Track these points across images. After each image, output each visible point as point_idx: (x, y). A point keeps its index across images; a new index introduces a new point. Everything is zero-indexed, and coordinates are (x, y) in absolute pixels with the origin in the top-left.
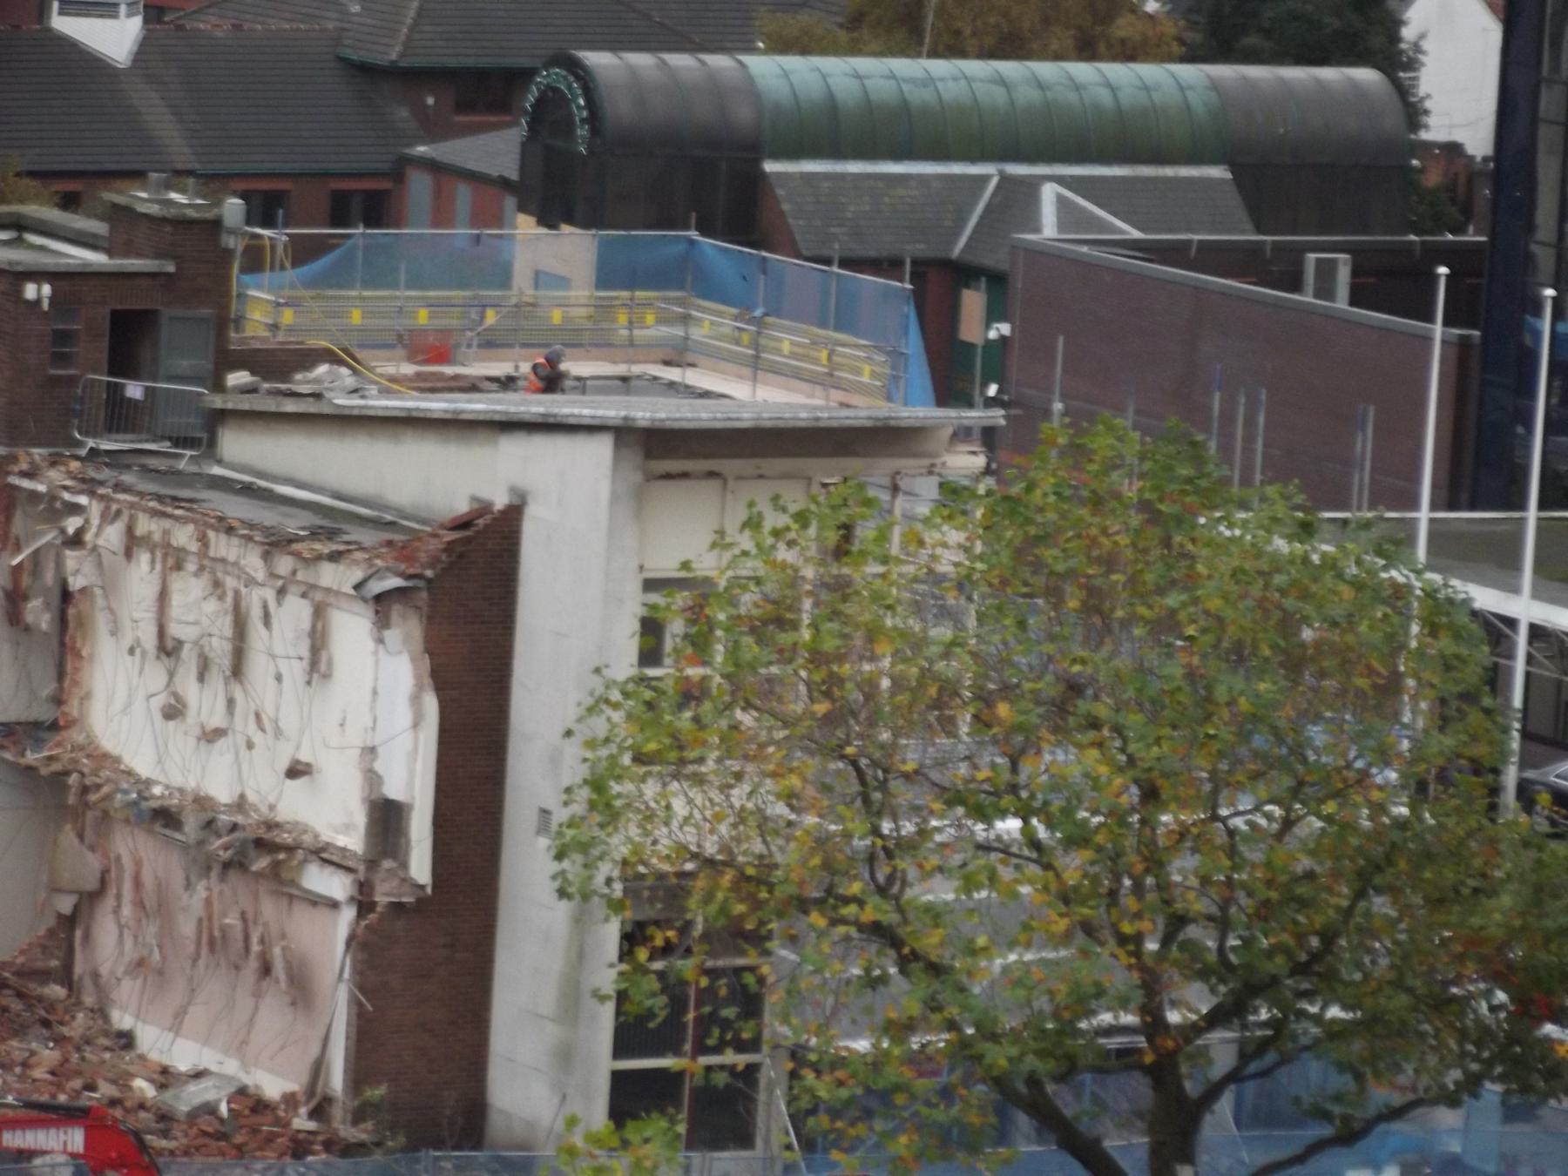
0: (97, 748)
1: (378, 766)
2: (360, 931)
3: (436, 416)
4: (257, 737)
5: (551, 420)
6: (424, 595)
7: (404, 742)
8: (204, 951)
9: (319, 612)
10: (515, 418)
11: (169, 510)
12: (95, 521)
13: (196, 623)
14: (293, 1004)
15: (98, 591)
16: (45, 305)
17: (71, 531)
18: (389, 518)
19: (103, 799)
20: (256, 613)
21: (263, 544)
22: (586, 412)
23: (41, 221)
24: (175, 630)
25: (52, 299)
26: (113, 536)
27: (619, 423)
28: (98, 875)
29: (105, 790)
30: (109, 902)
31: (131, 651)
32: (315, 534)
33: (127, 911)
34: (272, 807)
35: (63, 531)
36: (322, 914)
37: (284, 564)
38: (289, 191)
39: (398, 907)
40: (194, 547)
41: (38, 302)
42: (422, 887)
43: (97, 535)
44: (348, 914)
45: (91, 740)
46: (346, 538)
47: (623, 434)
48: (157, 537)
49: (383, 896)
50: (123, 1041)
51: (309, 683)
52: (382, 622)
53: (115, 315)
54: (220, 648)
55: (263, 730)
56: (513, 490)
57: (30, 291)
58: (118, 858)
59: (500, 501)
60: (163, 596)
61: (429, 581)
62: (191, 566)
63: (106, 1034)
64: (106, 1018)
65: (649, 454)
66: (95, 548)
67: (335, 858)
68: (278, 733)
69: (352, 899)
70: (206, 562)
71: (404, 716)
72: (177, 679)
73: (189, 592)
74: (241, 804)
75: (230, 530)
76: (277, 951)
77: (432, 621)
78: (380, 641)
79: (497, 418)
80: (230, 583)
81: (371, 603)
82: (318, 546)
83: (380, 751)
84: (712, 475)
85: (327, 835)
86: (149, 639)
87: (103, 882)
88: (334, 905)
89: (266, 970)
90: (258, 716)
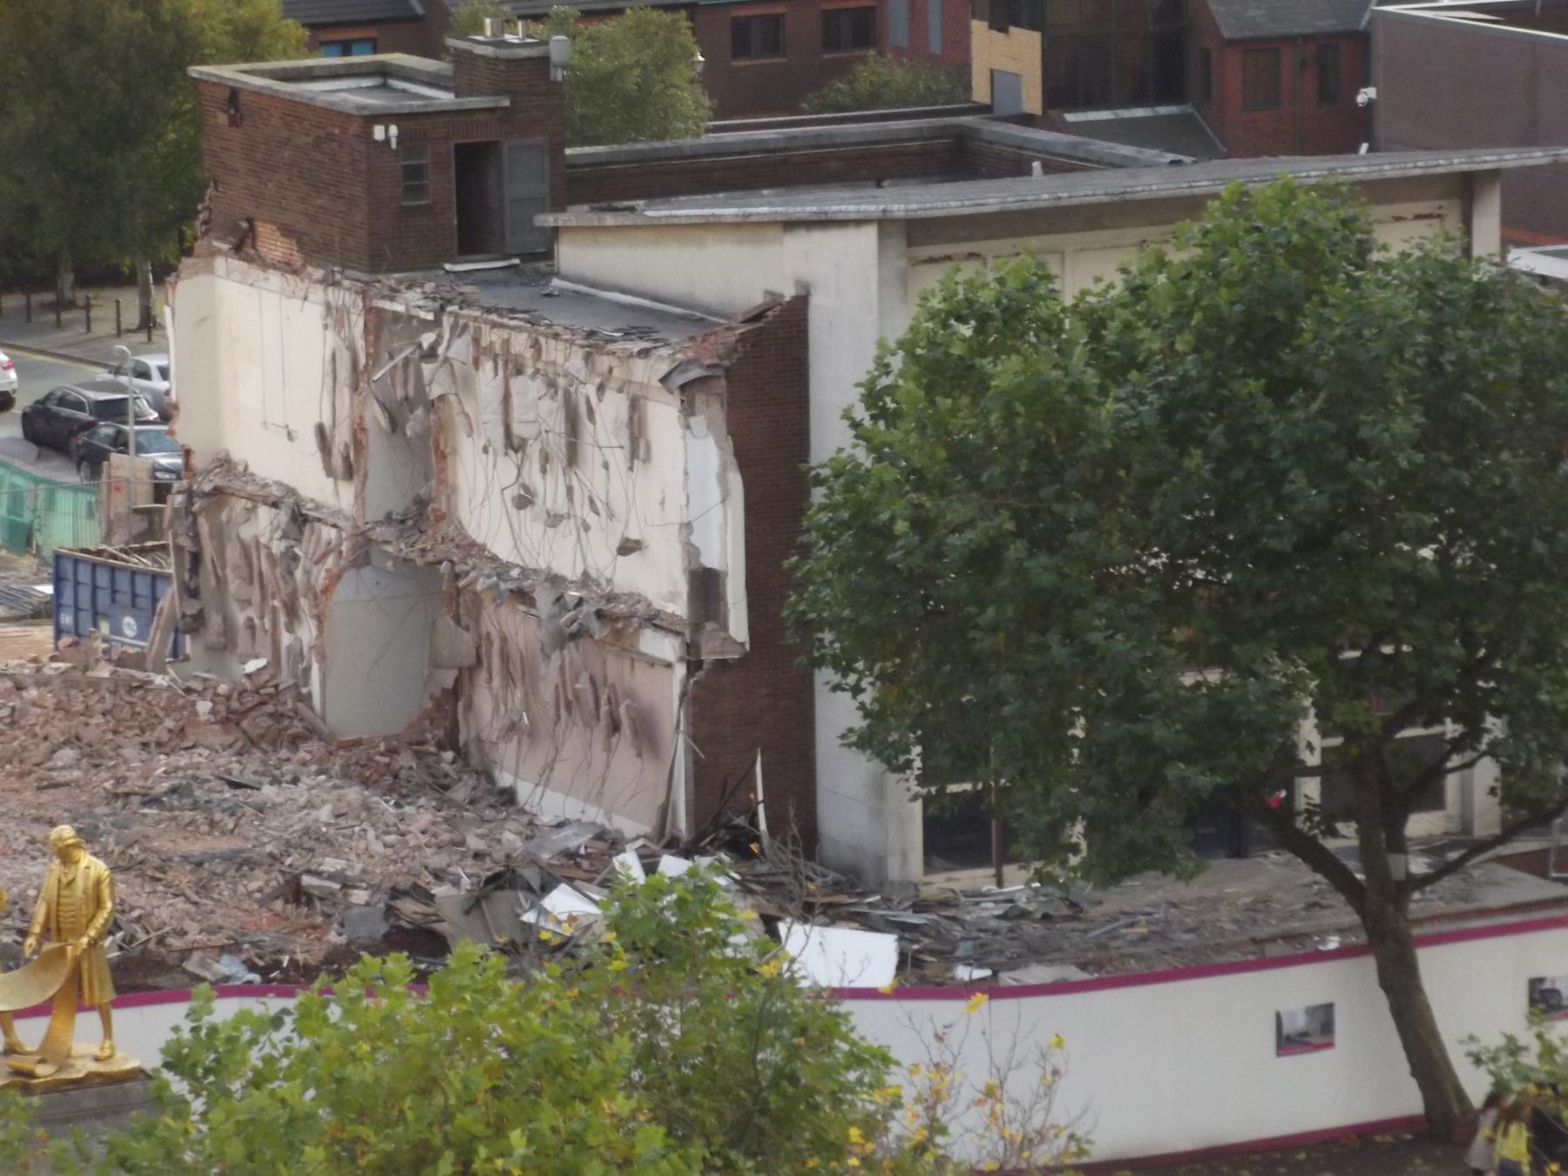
0: (466, 537)
1: (694, 539)
2: (690, 688)
3: (729, 220)
4: (592, 519)
5: (823, 217)
6: (723, 382)
7: (717, 515)
8: (563, 713)
9: (635, 405)
10: (794, 218)
11: (506, 321)
12: (447, 336)
13: (535, 421)
14: (639, 755)
15: (452, 398)
16: (394, 145)
17: (425, 345)
18: (699, 315)
19: (470, 584)
20: (583, 409)
21: (582, 347)
22: (852, 208)
23: (403, 68)
24: (518, 430)
25: (400, 138)
26: (460, 349)
27: (879, 215)
28: (473, 653)
29: (473, 574)
30: (482, 676)
31: (485, 450)
32: (627, 334)
33: (496, 682)
34: (609, 581)
35: (420, 346)
36: (659, 671)
37: (603, 362)
38: (783, 15)
39: (722, 664)
40: (529, 354)
41: (387, 140)
42: (742, 644)
43: (448, 348)
44: (680, 670)
45: (460, 528)
46: (655, 336)
47: (885, 224)
48: (498, 348)
49: (708, 657)
50: (505, 797)
51: (631, 468)
52: (688, 410)
53: (459, 149)
54: (557, 444)
55: (598, 514)
56: (799, 283)
57: (379, 132)
58: (488, 635)
59: (789, 292)
60: (506, 399)
61: (727, 370)
62: (530, 371)
63: (490, 792)
64: (490, 779)
65: (911, 242)
66: (447, 360)
67: (665, 624)
68: (611, 516)
69: (681, 659)
70: (540, 365)
71: (715, 493)
72: (525, 471)
73: (527, 390)
74: (586, 580)
75: (556, 336)
76: (622, 710)
77: (733, 406)
78: (688, 427)
79: (779, 218)
80: (562, 382)
81: (677, 393)
82: (629, 345)
83: (695, 525)
84: (972, 256)
85: (658, 604)
86: (498, 434)
87: (478, 657)
88: (669, 665)
89: (615, 727)
90: (591, 501)
